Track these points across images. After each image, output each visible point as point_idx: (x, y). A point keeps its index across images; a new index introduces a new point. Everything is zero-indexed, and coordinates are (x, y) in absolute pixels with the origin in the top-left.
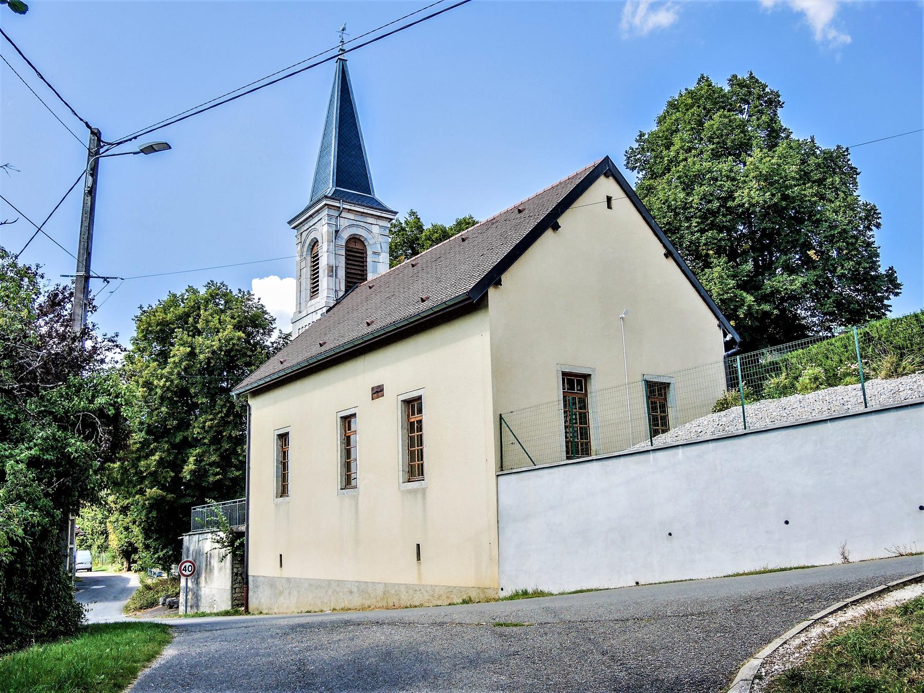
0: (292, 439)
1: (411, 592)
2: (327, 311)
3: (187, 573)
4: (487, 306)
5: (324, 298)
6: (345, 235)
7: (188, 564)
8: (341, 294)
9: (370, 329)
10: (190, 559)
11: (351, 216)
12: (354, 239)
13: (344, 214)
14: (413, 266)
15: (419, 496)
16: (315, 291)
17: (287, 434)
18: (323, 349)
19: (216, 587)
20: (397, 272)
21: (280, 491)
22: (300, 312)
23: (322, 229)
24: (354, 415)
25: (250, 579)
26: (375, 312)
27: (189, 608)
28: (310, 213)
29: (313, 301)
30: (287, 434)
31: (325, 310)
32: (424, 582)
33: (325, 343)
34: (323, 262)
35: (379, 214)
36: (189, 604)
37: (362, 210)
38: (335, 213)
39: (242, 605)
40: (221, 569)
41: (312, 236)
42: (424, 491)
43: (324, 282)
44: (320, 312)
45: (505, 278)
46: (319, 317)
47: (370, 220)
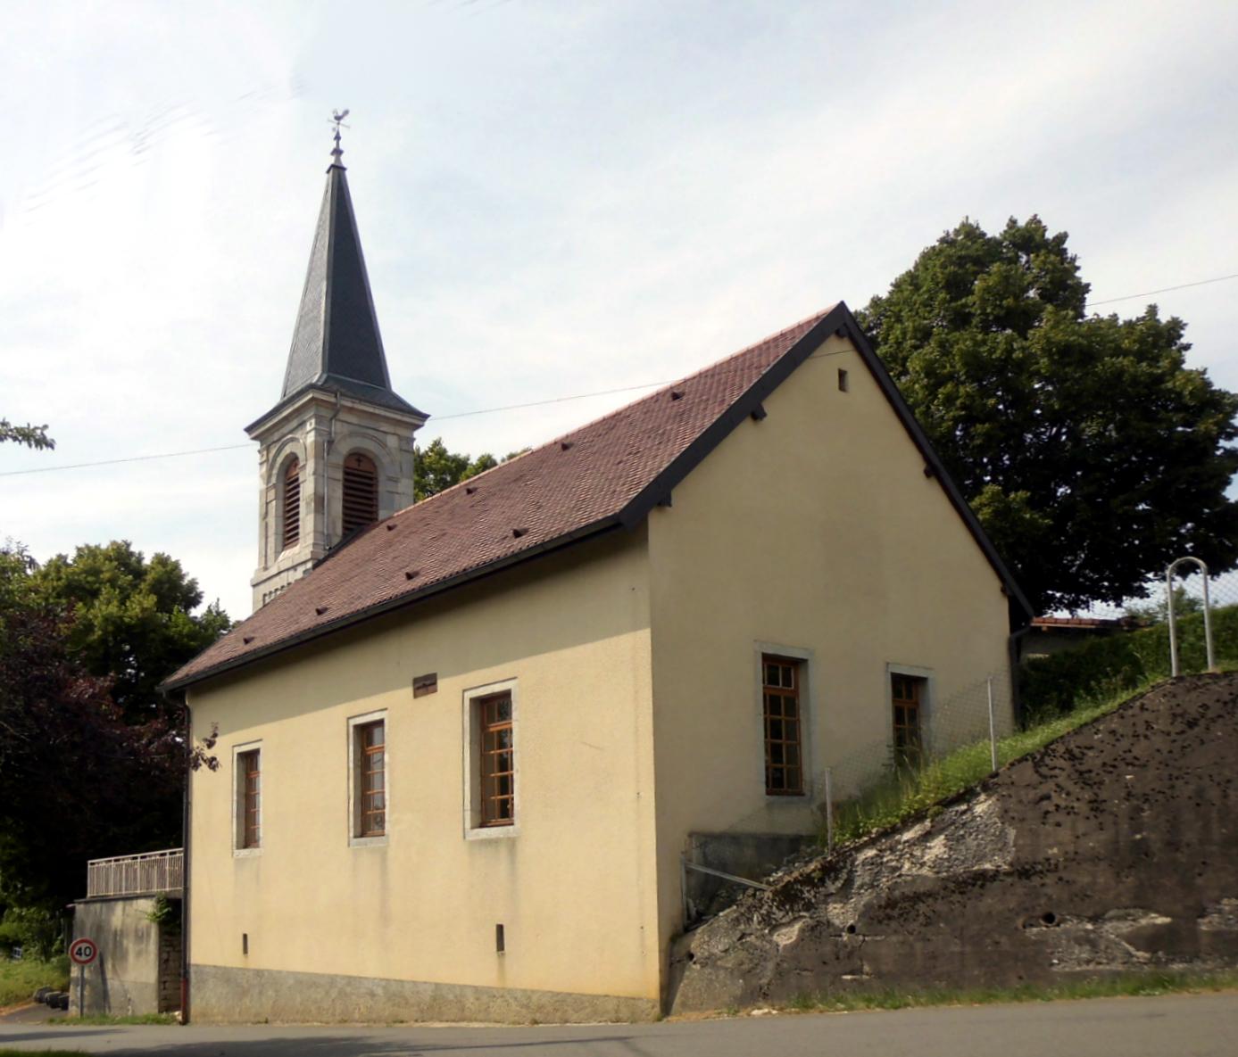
0: (263, 763)
1: (485, 998)
2: (315, 567)
3: (84, 958)
4: (645, 539)
5: (303, 549)
6: (344, 448)
7: (84, 945)
8: (336, 540)
9: (248, 648)
10: (87, 937)
11: (354, 419)
12: (358, 456)
13: (343, 416)
14: (469, 492)
15: (503, 851)
16: (289, 535)
17: (255, 753)
18: (324, 618)
19: (138, 972)
20: (438, 504)
21: (242, 839)
22: (266, 569)
23: (308, 437)
24: (380, 723)
25: (192, 970)
26: (375, 575)
27: (85, 1010)
28: (285, 414)
29: (288, 553)
30: (255, 753)
31: (309, 565)
32: (510, 984)
33: (326, 609)
34: (307, 489)
35: (398, 417)
36: (86, 1003)
37: (371, 410)
38: (327, 413)
39: (176, 1008)
40: (139, 954)
41: (287, 450)
42: (512, 843)
43: (307, 521)
44: (301, 569)
45: (677, 494)
46: (299, 574)
47: (385, 427)
